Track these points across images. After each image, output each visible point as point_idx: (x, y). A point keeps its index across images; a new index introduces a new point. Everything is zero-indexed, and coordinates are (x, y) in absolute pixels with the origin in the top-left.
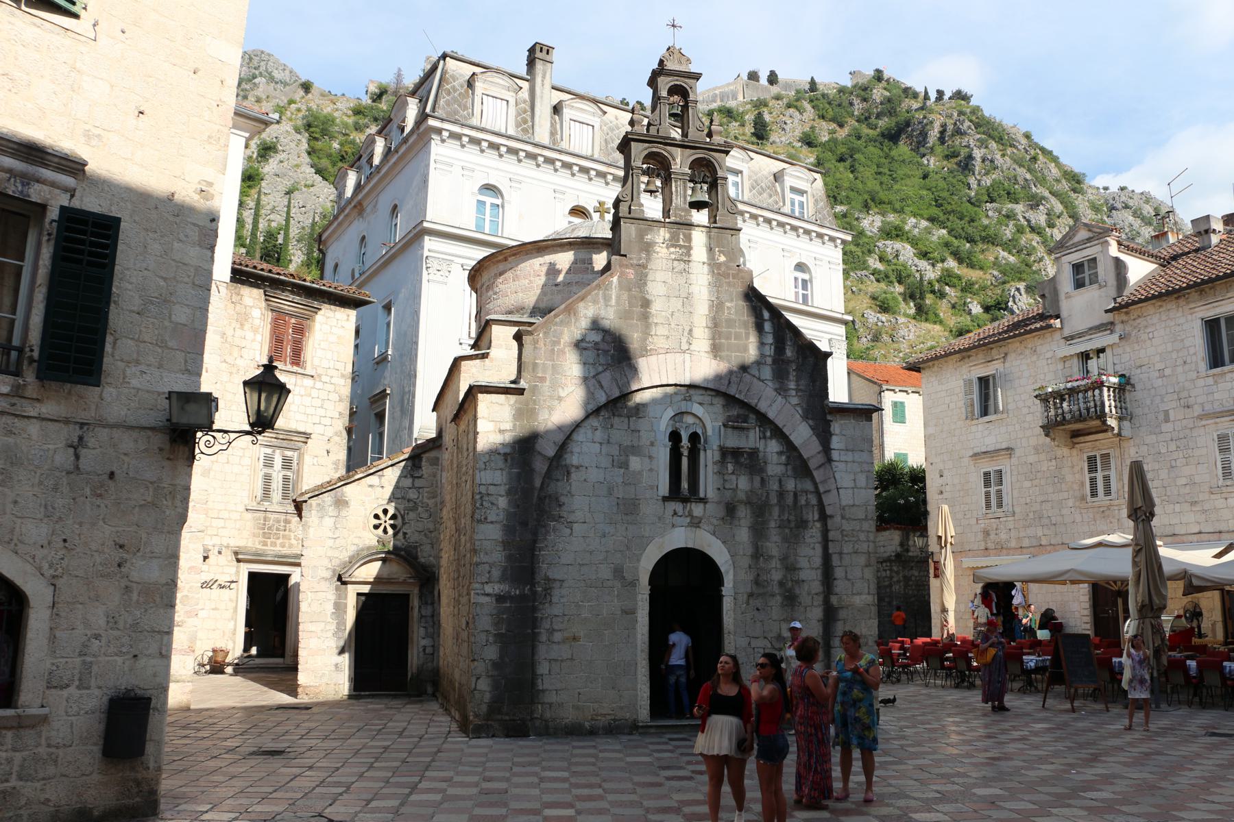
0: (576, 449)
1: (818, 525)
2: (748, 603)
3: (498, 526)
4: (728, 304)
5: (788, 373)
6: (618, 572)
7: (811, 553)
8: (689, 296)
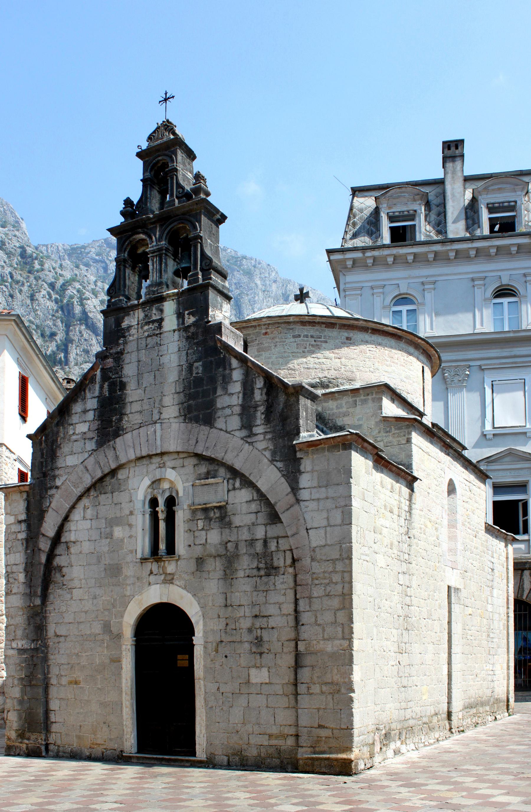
0: (73, 528)
2: (217, 651)
3: (19, 596)
4: (196, 364)
5: (255, 417)
6: (107, 627)
7: (282, 599)
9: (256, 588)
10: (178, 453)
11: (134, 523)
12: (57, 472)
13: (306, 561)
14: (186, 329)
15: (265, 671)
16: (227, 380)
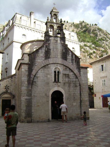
1: (79, 86)
2: (67, 100)
6: (46, 95)
8: (57, 48)
9: (74, 89)
10: (60, 64)
11: (52, 75)
12: (35, 62)
13: (82, 85)
14: (62, 43)
15: (75, 103)
16: (69, 54)
